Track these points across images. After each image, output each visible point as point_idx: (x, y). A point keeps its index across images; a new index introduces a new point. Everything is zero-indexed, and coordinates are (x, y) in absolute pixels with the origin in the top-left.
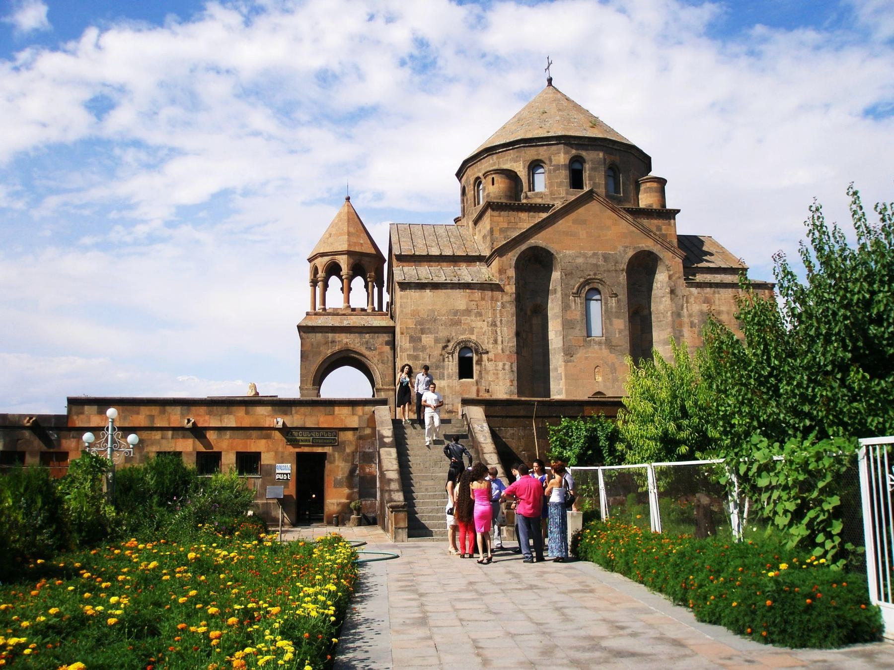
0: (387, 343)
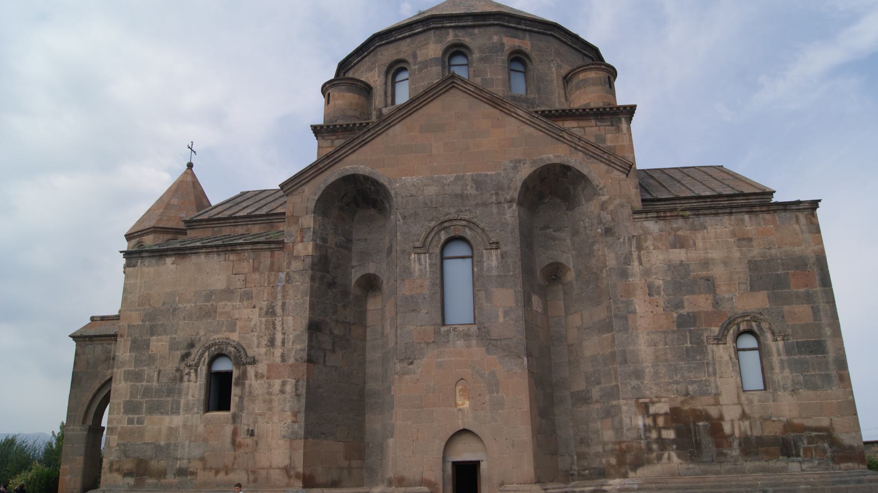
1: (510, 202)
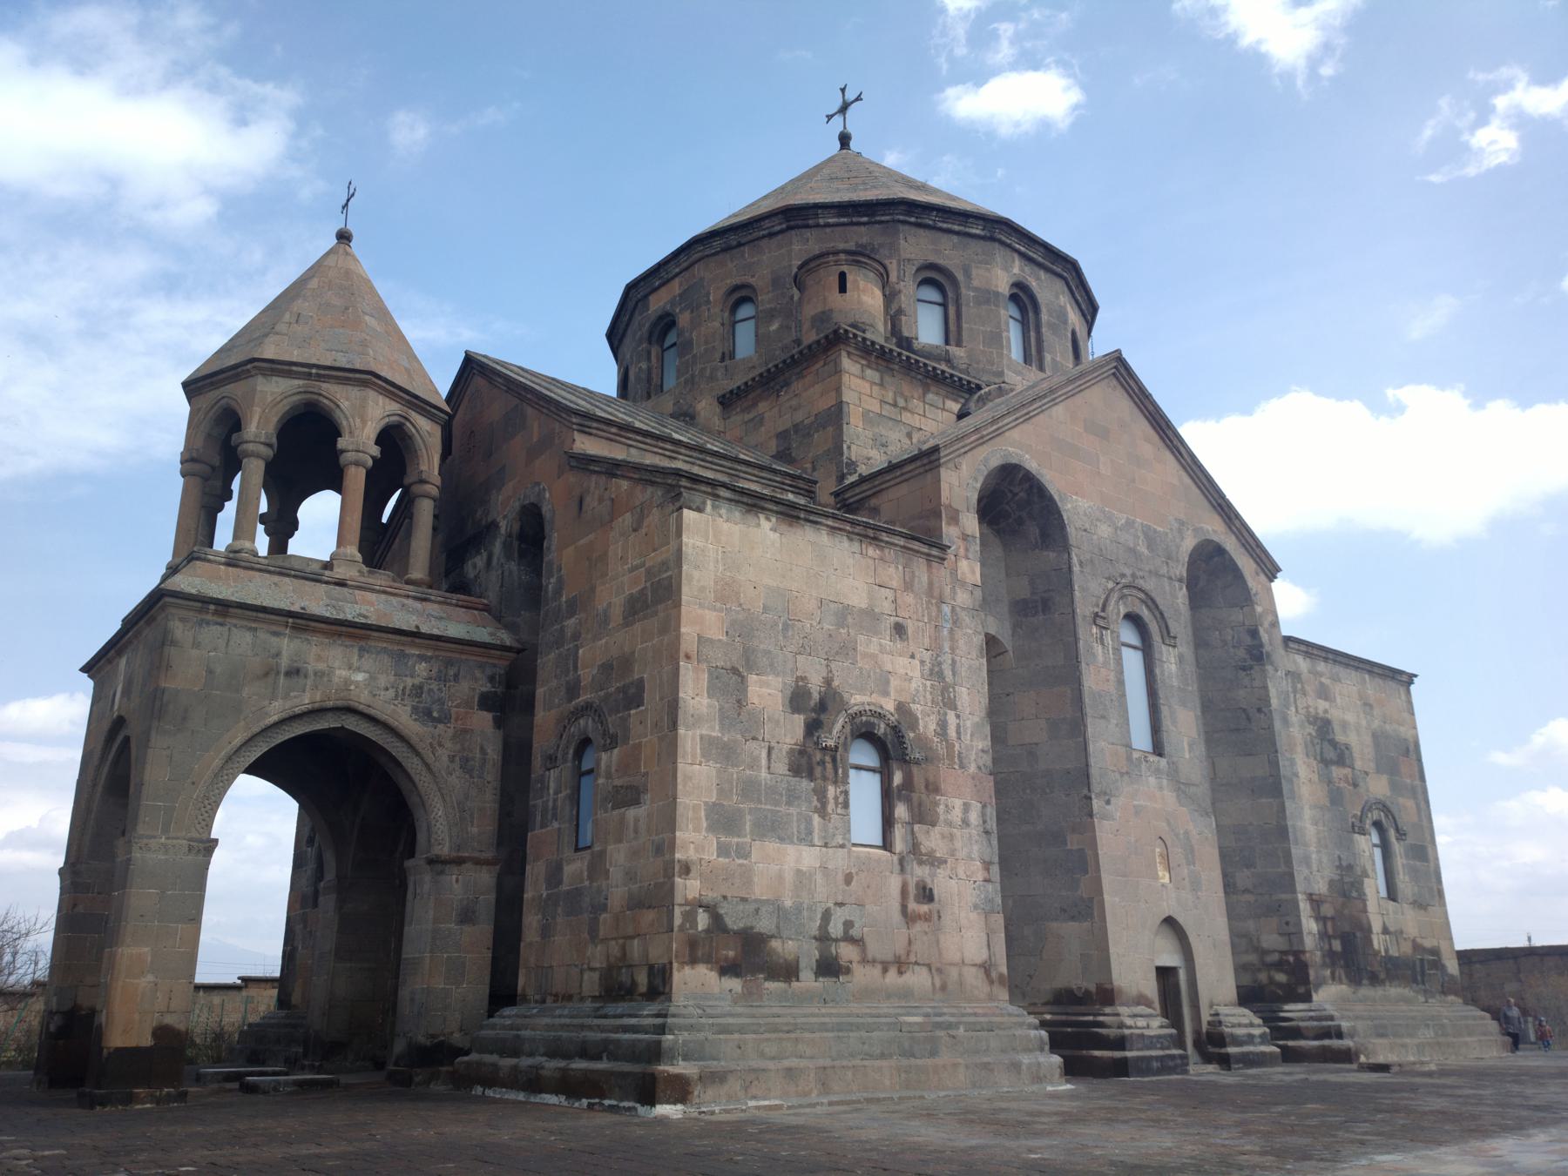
0: (486, 702)
1: (1180, 580)
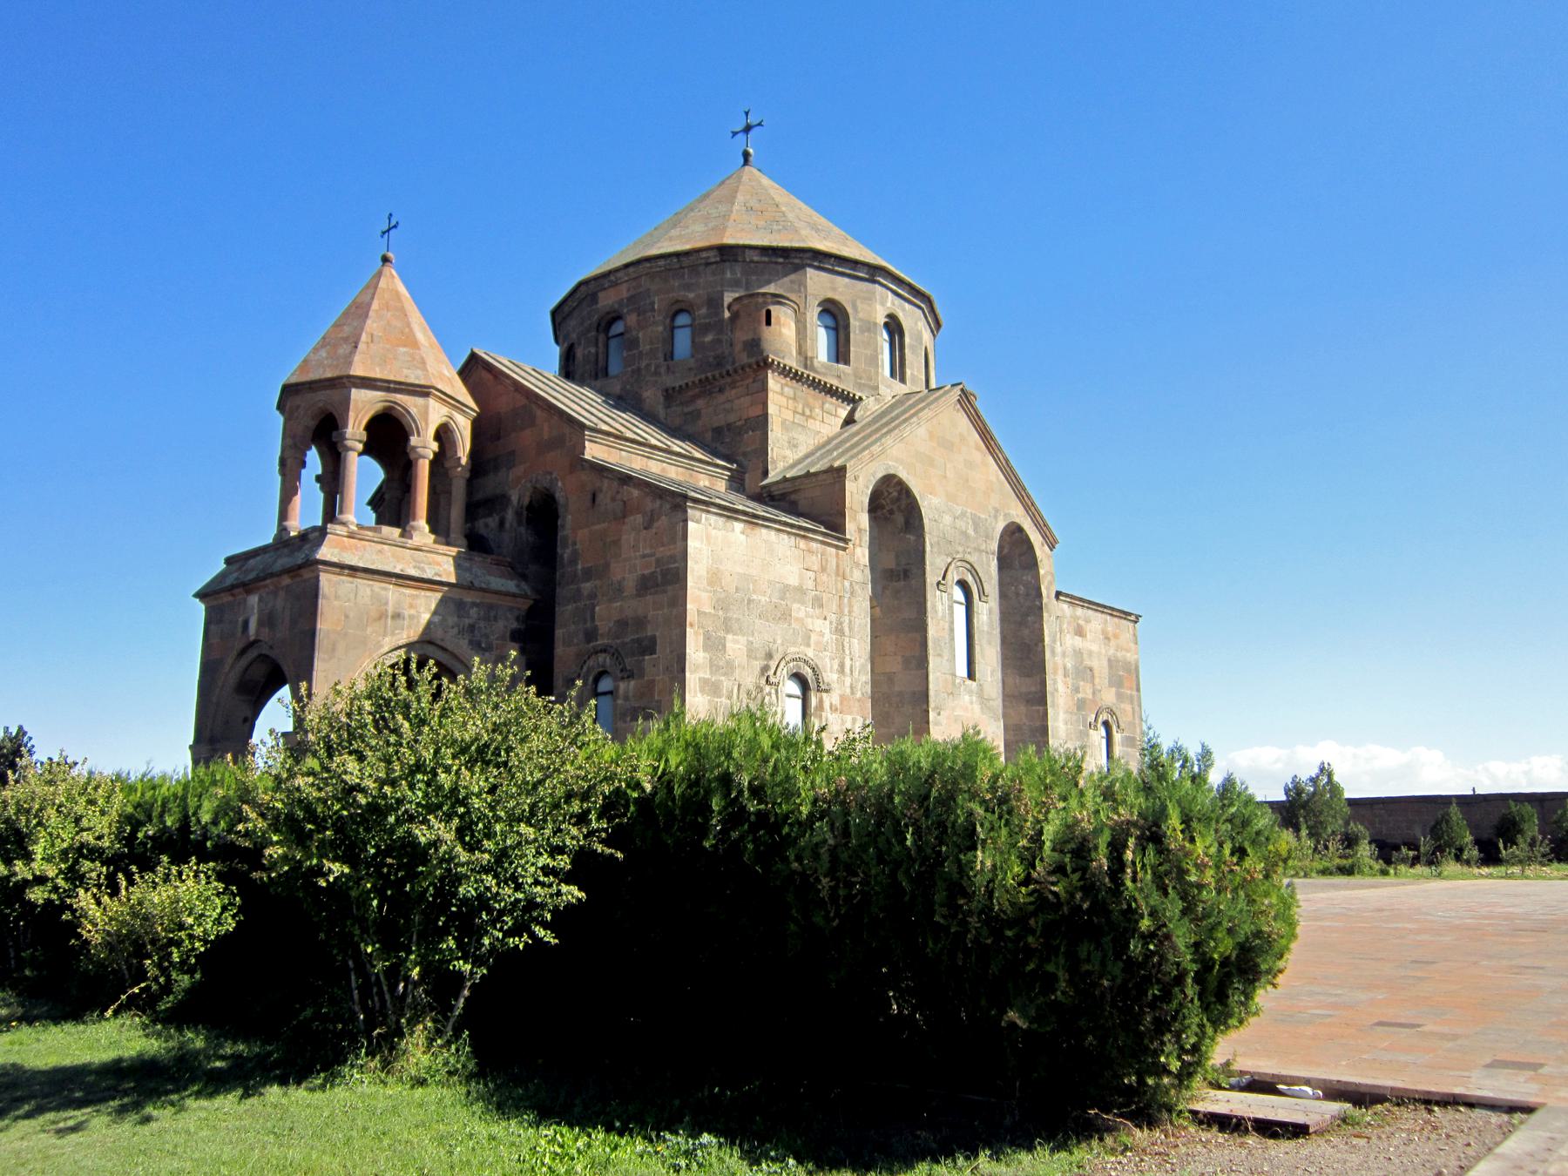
0: (516, 637)
